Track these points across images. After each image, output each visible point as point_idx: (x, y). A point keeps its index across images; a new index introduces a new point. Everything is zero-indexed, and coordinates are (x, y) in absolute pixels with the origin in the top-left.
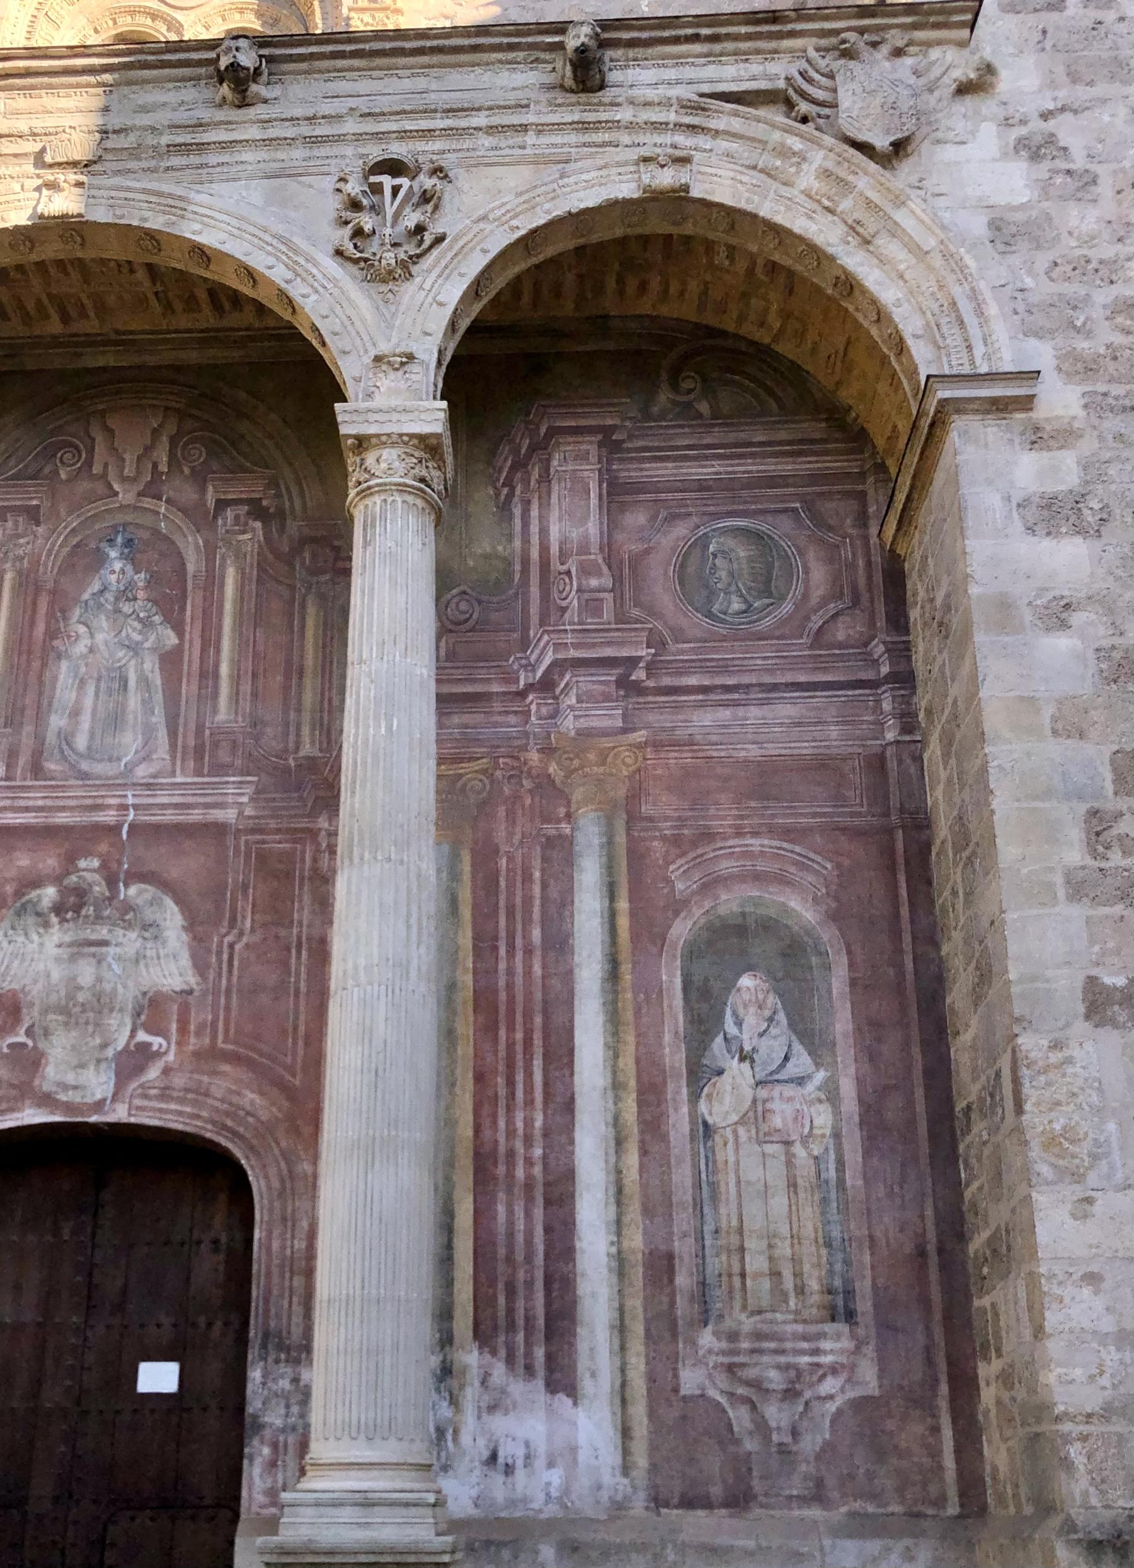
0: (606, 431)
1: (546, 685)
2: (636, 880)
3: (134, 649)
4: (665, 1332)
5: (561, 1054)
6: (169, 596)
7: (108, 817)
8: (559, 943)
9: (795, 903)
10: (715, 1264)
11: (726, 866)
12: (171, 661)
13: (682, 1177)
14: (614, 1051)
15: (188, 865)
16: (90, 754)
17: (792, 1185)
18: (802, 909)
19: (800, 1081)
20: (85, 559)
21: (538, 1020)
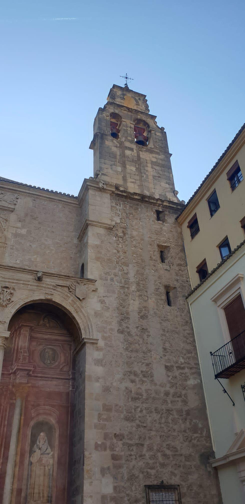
0: (31, 327)
1: (15, 373)
2: (25, 413)
5: (7, 448)
8: (10, 425)
9: (52, 419)
10: (29, 491)
11: (41, 411)
13: (26, 473)
14: (17, 447)
17: (45, 475)
18: (53, 421)
19: (48, 454)
21: (4, 440)
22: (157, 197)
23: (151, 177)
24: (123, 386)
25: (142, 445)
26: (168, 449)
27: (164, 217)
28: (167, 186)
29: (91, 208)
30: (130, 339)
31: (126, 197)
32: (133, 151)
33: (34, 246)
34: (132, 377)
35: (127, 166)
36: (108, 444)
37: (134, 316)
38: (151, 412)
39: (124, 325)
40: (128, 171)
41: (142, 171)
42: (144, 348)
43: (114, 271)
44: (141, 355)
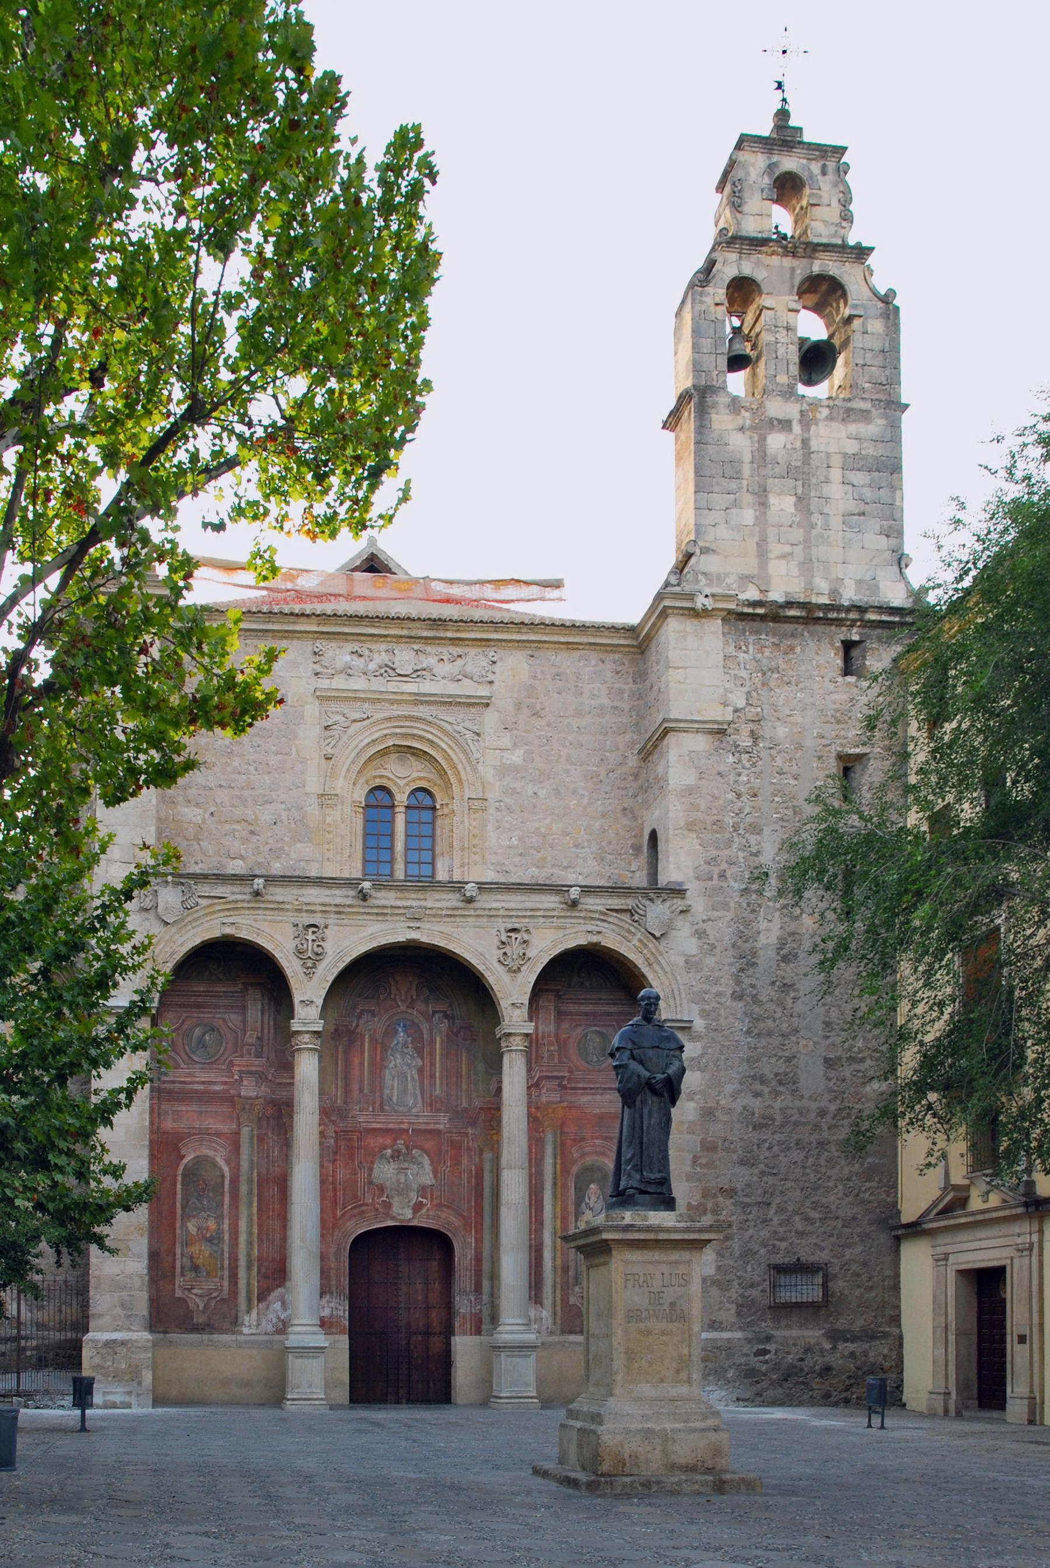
0: (558, 991)
3: (409, 1065)
4: (566, 1289)
6: (420, 1047)
7: (405, 1126)
12: (421, 1071)
14: (554, 1205)
15: (429, 1144)
16: (398, 1104)
20: (391, 1032)
22: (849, 595)
23: (836, 523)
24: (738, 1106)
25: (769, 1204)
26: (814, 1209)
27: (864, 658)
28: (883, 542)
29: (674, 677)
30: (757, 1010)
31: (763, 618)
32: (790, 430)
33: (542, 793)
34: (758, 1087)
35: (773, 499)
36: (710, 1205)
37: (767, 958)
38: (789, 1148)
39: (747, 981)
40: (773, 515)
41: (814, 504)
42: (784, 1026)
43: (727, 852)
44: (776, 1041)
